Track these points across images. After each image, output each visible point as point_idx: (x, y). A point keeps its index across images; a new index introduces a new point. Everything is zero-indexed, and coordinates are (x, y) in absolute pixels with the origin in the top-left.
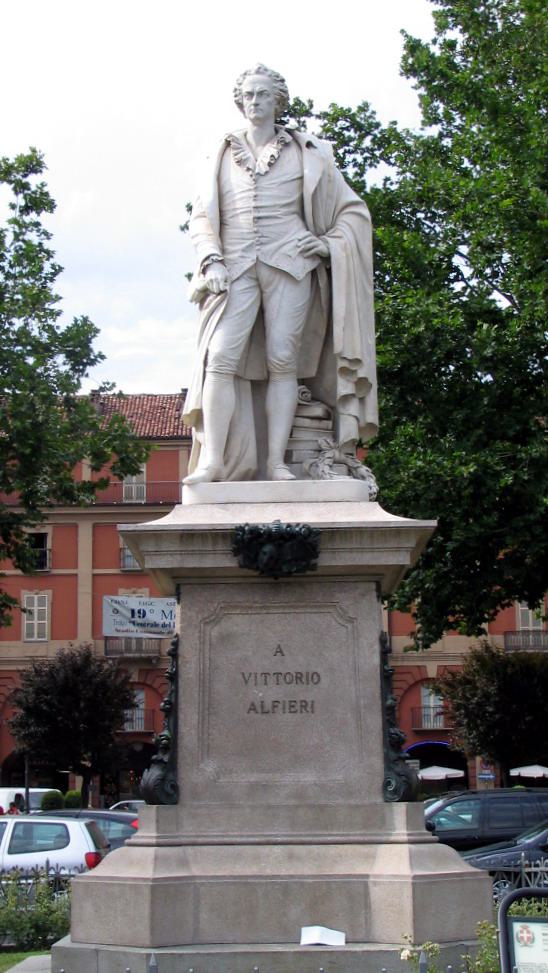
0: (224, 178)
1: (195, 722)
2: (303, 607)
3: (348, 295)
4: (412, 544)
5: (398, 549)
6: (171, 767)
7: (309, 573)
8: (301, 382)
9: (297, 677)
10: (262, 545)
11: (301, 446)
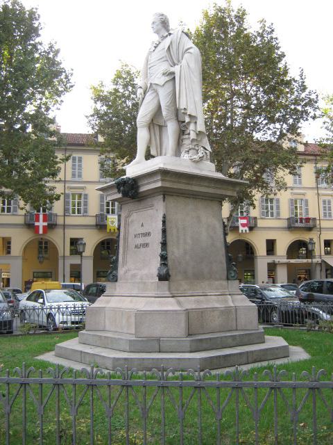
4: (159, 178)
5: (157, 181)
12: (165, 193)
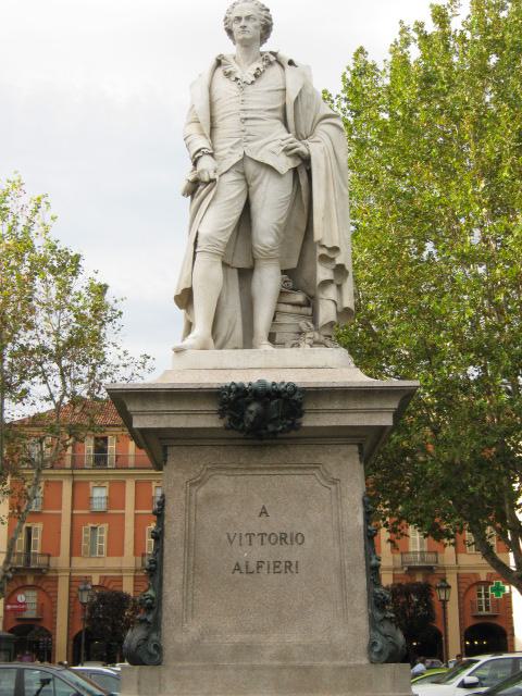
0: (214, 91)
1: (179, 582)
2: (287, 468)
3: (327, 190)
4: (394, 405)
5: (380, 411)
6: (155, 626)
7: (293, 433)
8: (284, 272)
9: (281, 538)
10: (249, 403)
11: (283, 329)
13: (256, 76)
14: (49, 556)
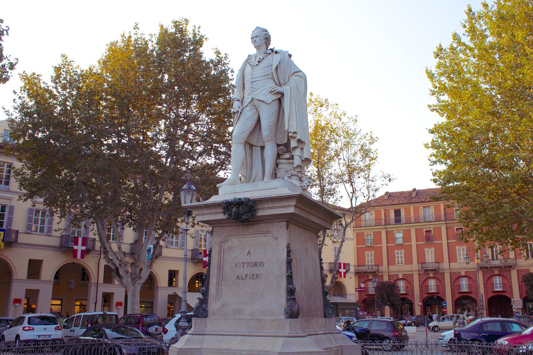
4: (294, 203)
5: (288, 206)
10: (232, 208)
12: (290, 220)
13: (258, 62)
14: (378, 266)
